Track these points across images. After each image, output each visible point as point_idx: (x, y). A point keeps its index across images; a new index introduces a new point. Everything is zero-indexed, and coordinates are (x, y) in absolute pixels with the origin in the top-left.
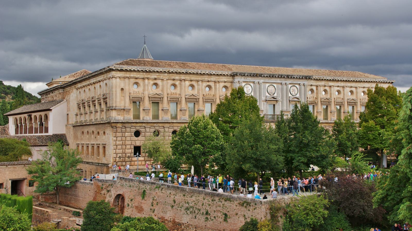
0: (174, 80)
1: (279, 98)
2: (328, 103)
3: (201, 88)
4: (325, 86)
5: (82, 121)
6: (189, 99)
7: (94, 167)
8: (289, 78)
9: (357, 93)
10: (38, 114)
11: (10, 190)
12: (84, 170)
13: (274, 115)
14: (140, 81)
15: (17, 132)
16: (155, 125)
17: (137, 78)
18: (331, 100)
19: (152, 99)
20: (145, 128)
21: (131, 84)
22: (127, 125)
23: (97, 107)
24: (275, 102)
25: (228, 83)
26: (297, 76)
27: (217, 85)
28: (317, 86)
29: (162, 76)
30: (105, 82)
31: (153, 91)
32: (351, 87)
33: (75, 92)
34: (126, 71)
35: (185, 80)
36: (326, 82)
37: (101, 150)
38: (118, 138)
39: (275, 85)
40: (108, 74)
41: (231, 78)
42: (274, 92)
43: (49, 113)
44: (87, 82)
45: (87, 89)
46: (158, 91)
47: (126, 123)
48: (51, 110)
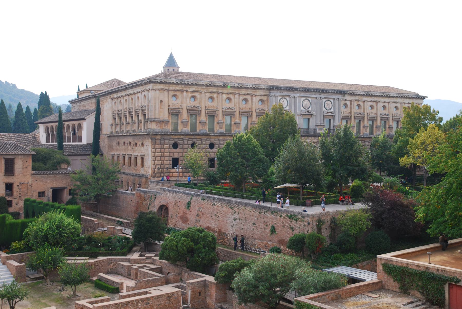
0: (212, 93)
1: (314, 113)
2: (361, 118)
3: (237, 101)
4: (359, 101)
5: (118, 131)
6: (226, 112)
7: (131, 177)
8: (324, 92)
9: (389, 108)
10: (71, 123)
11: (51, 199)
12: (120, 180)
13: (308, 129)
14: (178, 94)
15: (48, 141)
16: (193, 137)
17: (176, 91)
19: (190, 112)
20: (183, 140)
21: (170, 96)
22: (165, 137)
23: (135, 118)
24: (310, 116)
25: (264, 97)
26: (332, 90)
27: (254, 98)
29: (200, 89)
30: (143, 93)
31: (191, 103)
32: (384, 102)
33: (110, 102)
34: (166, 83)
35: (222, 93)
36: (360, 97)
37: (139, 161)
38: (157, 150)
39: (310, 99)
40: (147, 85)
41: (267, 91)
42: (308, 107)
43: (83, 123)
44: (124, 93)
45: (123, 100)
46: (196, 104)
47: (165, 135)
48: (85, 119)
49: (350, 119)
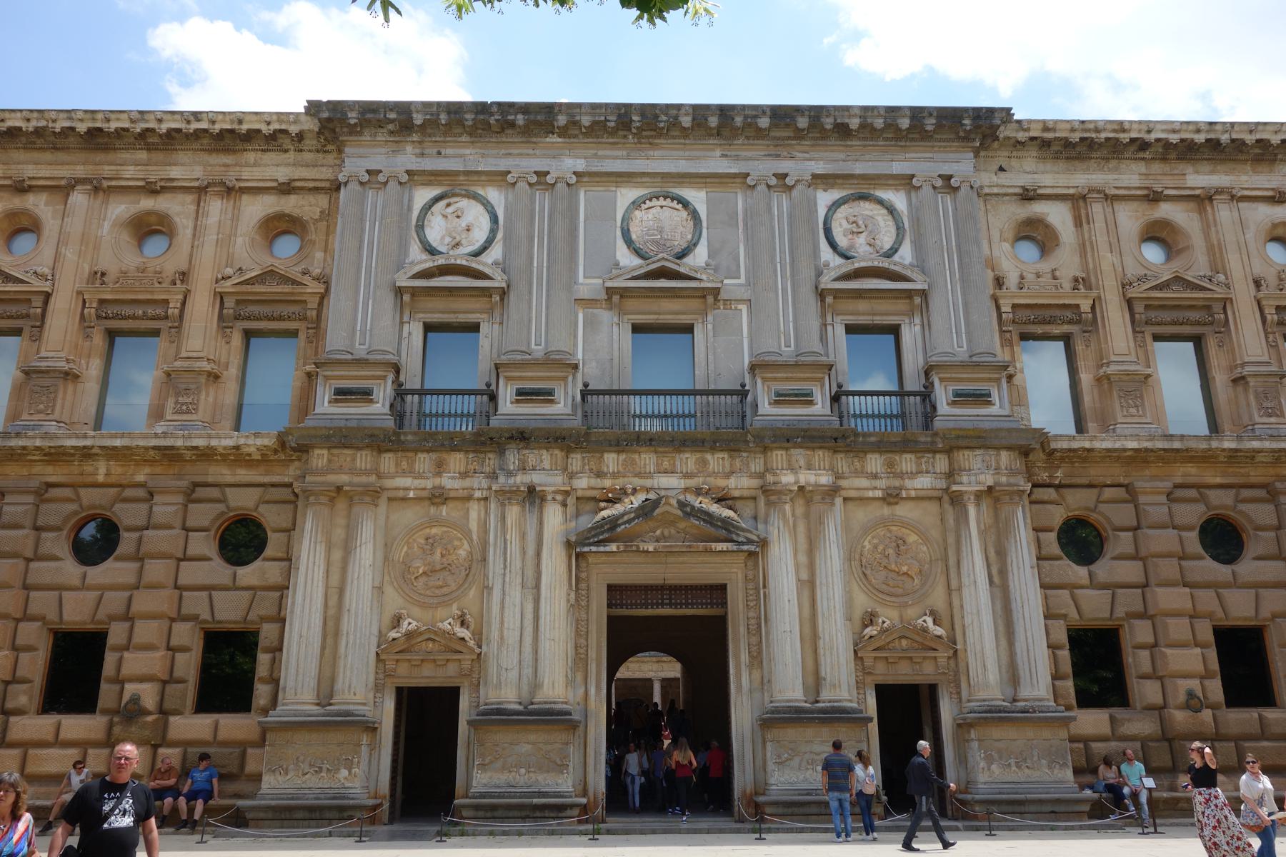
4: (1154, 198)
18: (1220, 293)
28: (1078, 201)
49: (1091, 323)
